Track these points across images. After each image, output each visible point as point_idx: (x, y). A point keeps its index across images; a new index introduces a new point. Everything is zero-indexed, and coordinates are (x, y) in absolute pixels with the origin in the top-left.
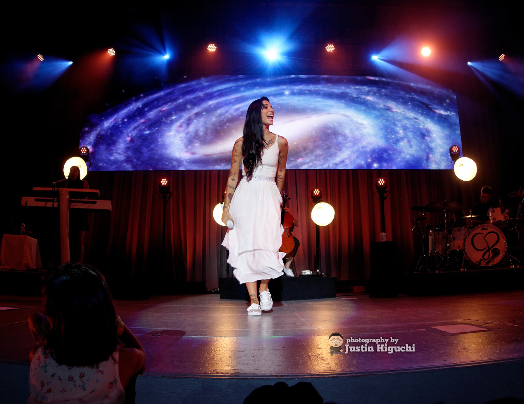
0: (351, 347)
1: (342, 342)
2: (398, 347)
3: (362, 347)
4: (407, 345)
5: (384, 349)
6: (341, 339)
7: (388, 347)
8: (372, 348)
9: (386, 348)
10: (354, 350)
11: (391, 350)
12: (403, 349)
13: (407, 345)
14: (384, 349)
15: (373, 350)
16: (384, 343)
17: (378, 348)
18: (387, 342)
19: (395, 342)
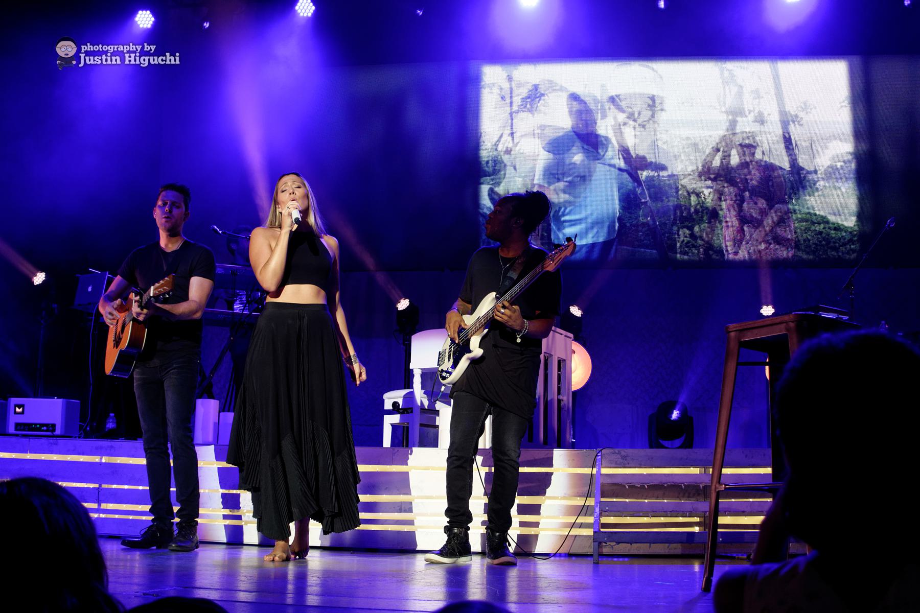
0: (87, 58)
2: (156, 58)
3: (104, 57)
7: (140, 57)
8: (118, 58)
9: (137, 58)
10: (92, 62)
11: (145, 62)
15: (119, 62)
17: (127, 59)
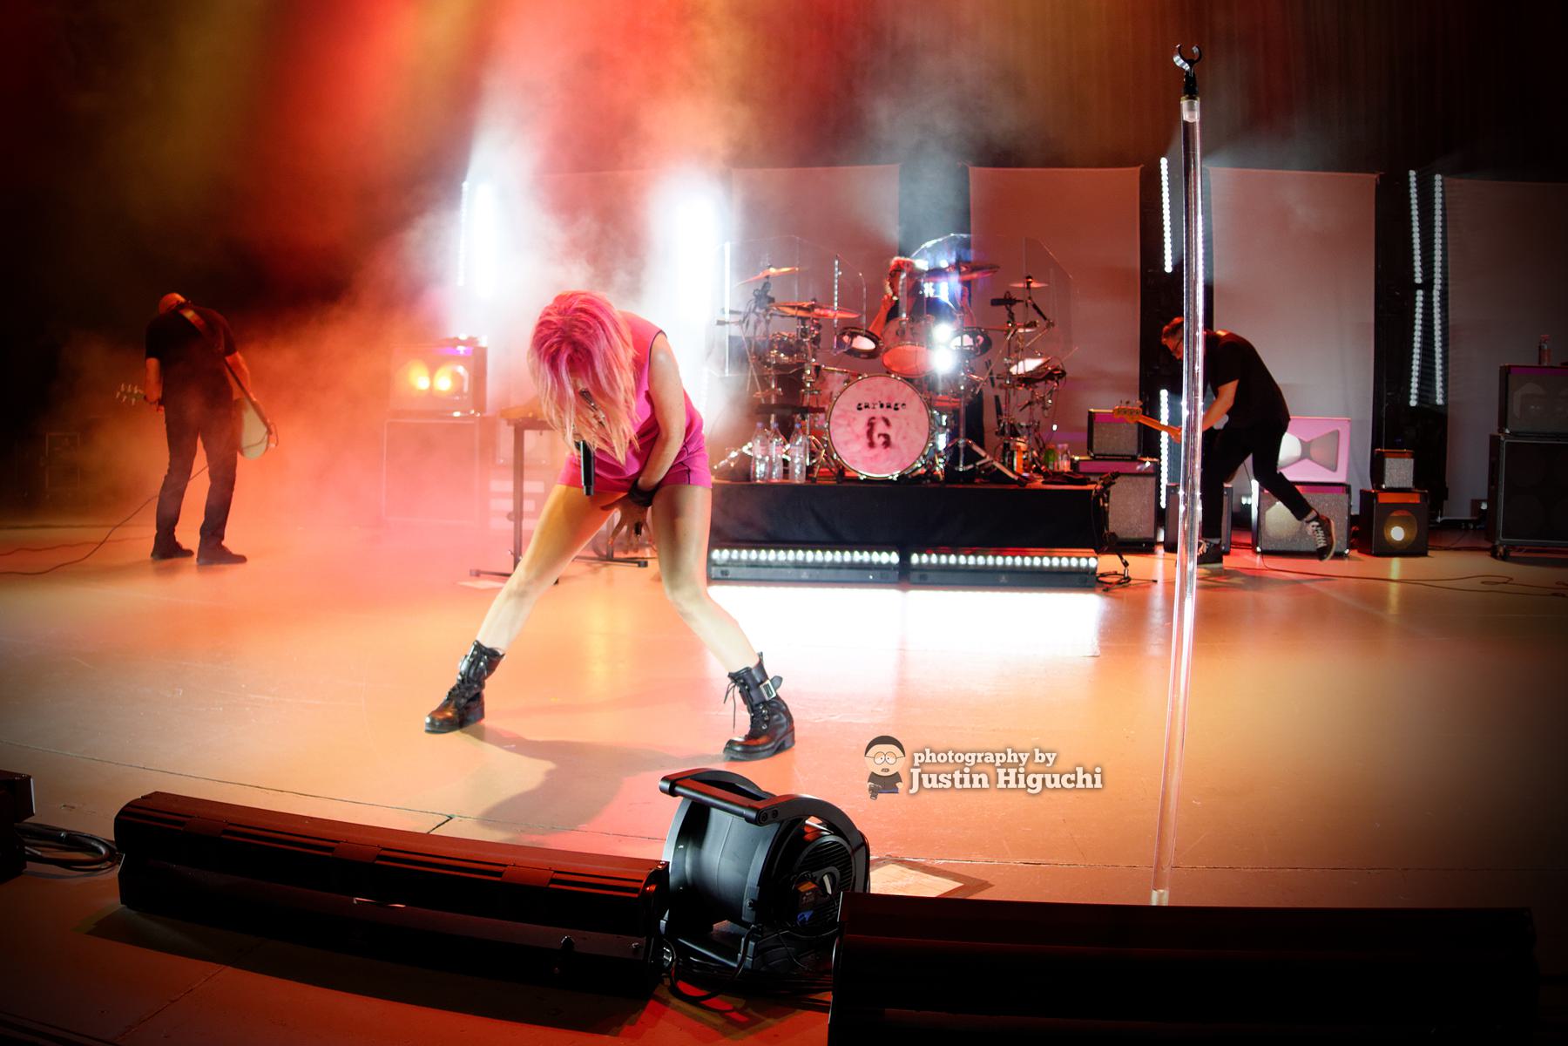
0: (925, 777)
4: (1080, 770)
5: (1017, 781)
8: (984, 777)
9: (1021, 777)
10: (934, 784)
12: (1069, 781)
13: (1080, 770)
14: (1017, 781)
15: (985, 785)
16: (1013, 765)
17: (1002, 778)
18: (1024, 760)
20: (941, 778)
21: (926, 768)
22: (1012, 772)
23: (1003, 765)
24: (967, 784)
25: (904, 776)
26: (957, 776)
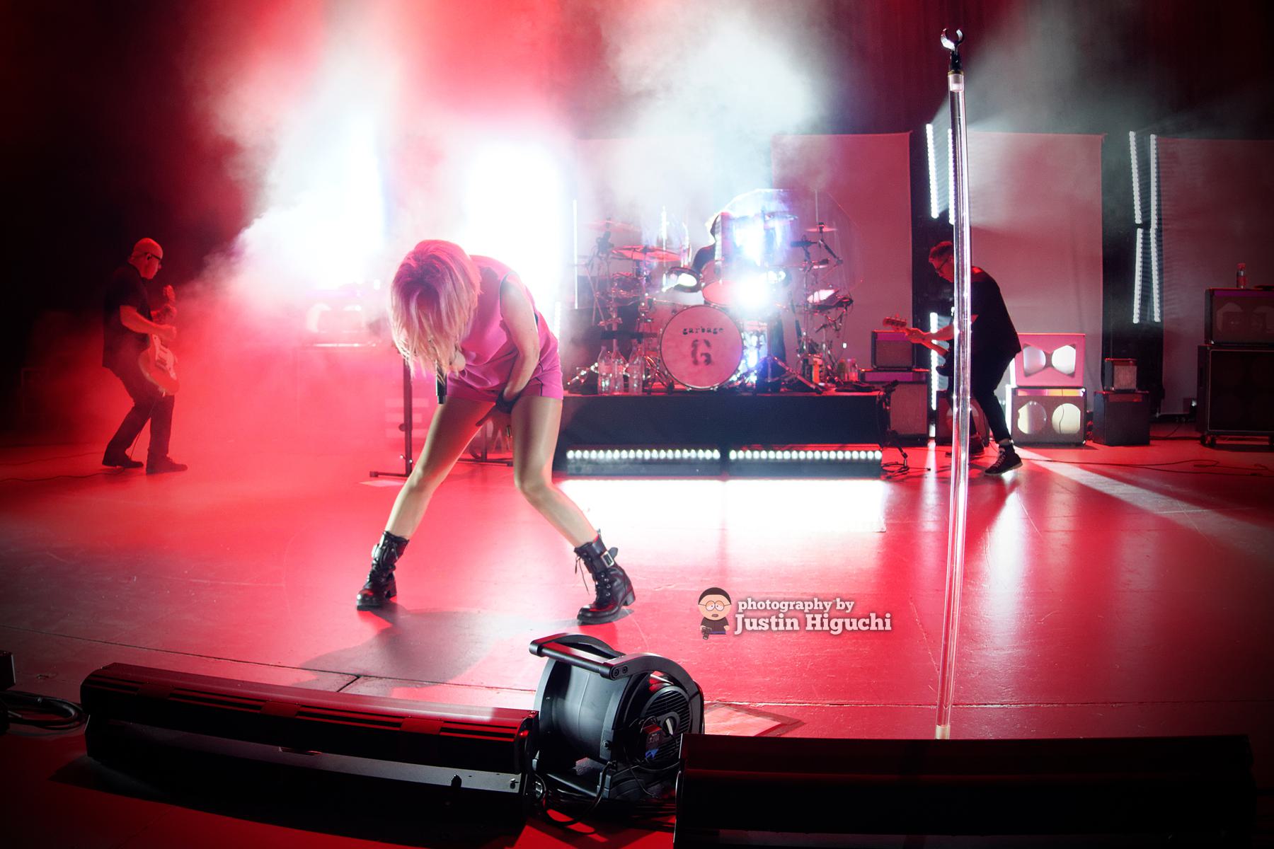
0: (747, 621)
1: (728, 608)
2: (854, 621)
4: (873, 615)
5: (822, 625)
6: (726, 601)
8: (795, 621)
9: (826, 621)
10: (755, 627)
12: (864, 624)
13: (873, 615)
14: (822, 625)
15: (796, 627)
16: (818, 612)
17: (810, 622)
18: (828, 608)
19: (846, 608)
20: (761, 622)
21: (749, 614)
22: (818, 617)
23: (811, 612)
24: (781, 627)
25: (730, 620)
26: (773, 620)
